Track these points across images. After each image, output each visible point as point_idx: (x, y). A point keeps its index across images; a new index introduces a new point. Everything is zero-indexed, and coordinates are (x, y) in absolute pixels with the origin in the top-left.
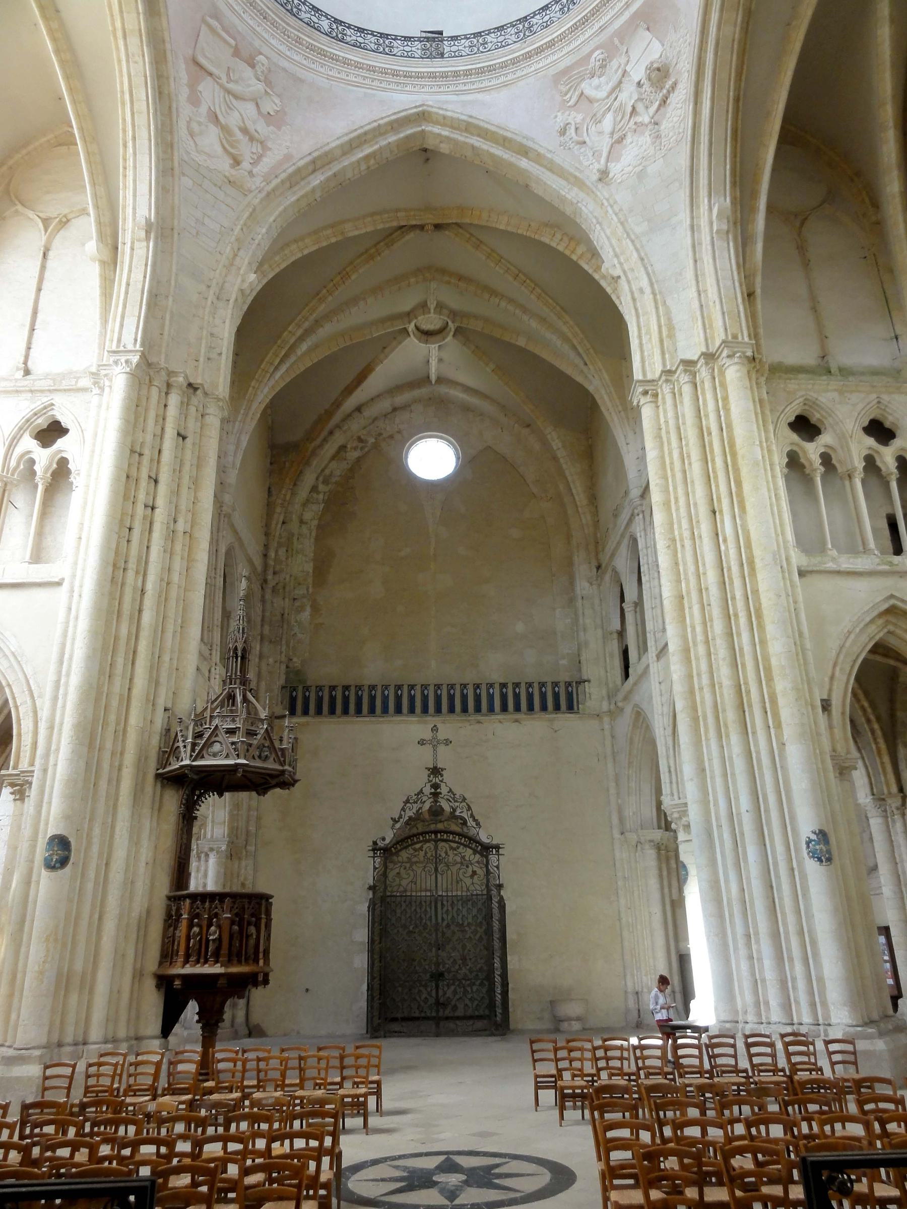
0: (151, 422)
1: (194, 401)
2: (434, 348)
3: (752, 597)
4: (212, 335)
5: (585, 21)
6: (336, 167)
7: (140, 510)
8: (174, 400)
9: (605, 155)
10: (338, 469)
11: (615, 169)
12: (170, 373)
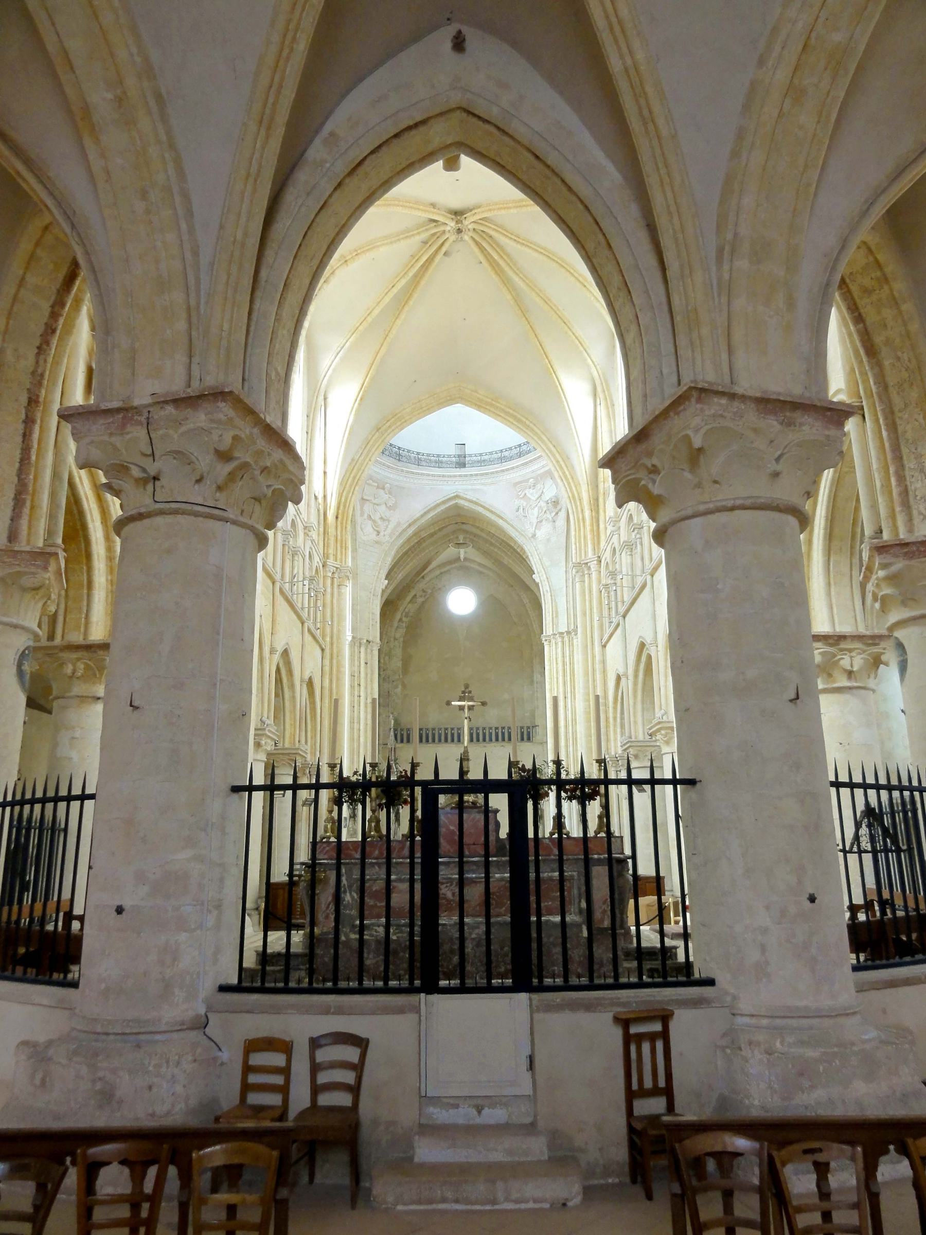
0: (356, 661)
1: (369, 646)
2: (462, 551)
3: (574, 733)
4: (373, 613)
5: (526, 463)
6: (418, 524)
7: (356, 698)
8: (363, 649)
9: (535, 525)
10: (412, 608)
11: (538, 534)
12: (360, 639)
